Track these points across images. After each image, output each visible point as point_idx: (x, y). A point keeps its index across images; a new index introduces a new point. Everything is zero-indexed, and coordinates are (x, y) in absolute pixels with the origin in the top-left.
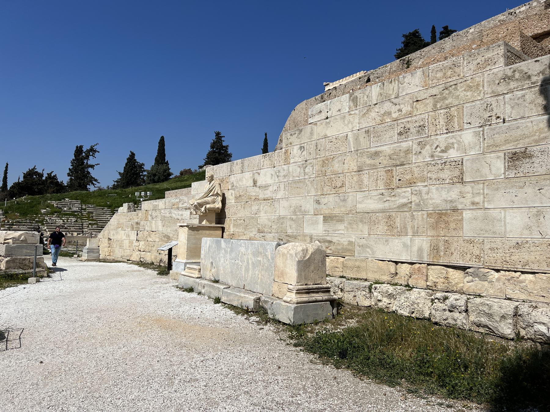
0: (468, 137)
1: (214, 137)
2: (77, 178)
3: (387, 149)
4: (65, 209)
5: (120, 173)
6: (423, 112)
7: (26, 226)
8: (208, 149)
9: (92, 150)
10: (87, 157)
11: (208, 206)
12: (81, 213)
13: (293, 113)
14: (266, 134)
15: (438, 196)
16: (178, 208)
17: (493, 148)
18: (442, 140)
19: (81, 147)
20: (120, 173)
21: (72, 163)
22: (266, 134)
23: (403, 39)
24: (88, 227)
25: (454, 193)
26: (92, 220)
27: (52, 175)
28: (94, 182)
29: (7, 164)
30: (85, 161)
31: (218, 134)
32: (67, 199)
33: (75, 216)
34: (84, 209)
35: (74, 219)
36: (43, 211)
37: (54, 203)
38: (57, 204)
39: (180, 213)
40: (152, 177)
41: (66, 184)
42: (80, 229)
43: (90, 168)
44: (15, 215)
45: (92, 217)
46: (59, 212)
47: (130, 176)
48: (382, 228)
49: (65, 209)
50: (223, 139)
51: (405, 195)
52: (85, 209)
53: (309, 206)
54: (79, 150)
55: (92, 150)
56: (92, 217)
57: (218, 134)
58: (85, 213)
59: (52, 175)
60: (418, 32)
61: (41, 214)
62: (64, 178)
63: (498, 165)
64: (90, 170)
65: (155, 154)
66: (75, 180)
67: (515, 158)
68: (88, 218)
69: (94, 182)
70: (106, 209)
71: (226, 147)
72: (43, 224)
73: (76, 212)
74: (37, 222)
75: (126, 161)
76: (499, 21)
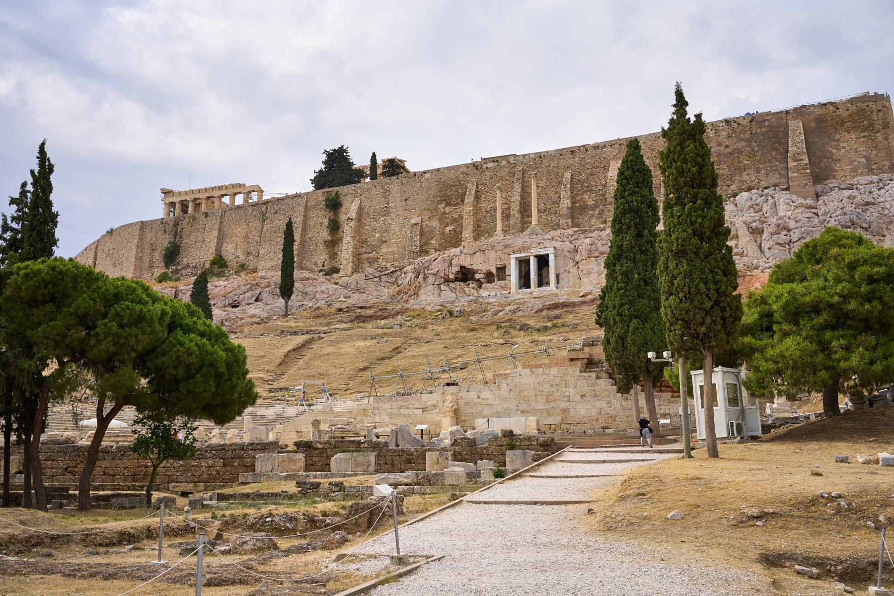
0: (571, 389)
3: (546, 390)
6: (558, 380)
15: (563, 405)
17: (577, 393)
18: (564, 389)
23: (324, 157)
25: (568, 404)
48: (545, 414)
51: (553, 404)
53: (513, 407)
60: (345, 151)
63: (579, 398)
67: (583, 396)
76: (462, 173)
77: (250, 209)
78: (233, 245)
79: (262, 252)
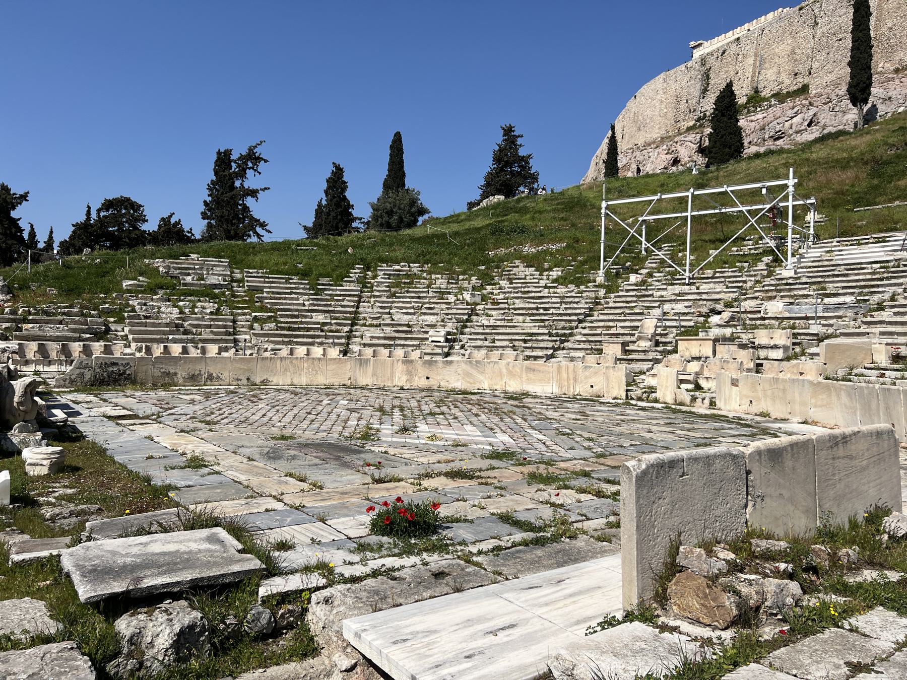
1: (499, 138)
2: (220, 219)
4: (189, 279)
5: (305, 228)
7: (67, 324)
8: (487, 164)
9: (252, 158)
10: (242, 174)
12: (231, 289)
13: (632, 105)
19: (228, 153)
20: (305, 228)
21: (209, 189)
24: (251, 328)
26: (263, 309)
27: (173, 221)
28: (259, 230)
29: (89, 207)
30: (237, 184)
31: (508, 131)
32: (193, 256)
33: (213, 297)
34: (238, 281)
35: (210, 307)
36: (126, 284)
37: (160, 265)
38: (168, 267)
40: (386, 218)
41: (198, 237)
42: (230, 334)
43: (249, 198)
44: (44, 294)
45: (261, 300)
46: (172, 288)
47: (335, 218)
49: (189, 279)
50: (519, 141)
52: (241, 281)
54: (223, 160)
55: (252, 158)
56: (261, 300)
57: (508, 131)
58: (240, 291)
59: (173, 221)
61: (120, 291)
62: (196, 225)
64: (250, 201)
65: (384, 173)
66: (219, 226)
68: (250, 304)
69: (259, 230)
70: (295, 279)
71: (526, 159)
72: (121, 320)
73: (215, 286)
74: (102, 313)
75: (325, 186)
78: (775, 70)
79: (816, 65)
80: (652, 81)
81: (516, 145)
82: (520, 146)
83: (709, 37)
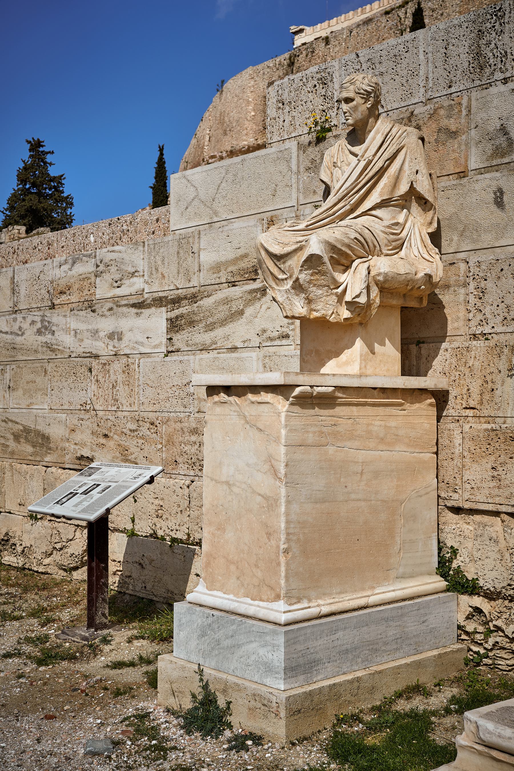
1: (25, 154)
8: (12, 185)
11: (382, 265)
14: (161, 149)
16: (91, 306)
22: (161, 149)
31: (36, 146)
39: (106, 325)
50: (49, 158)
57: (36, 146)
77: (384, 19)
80: (239, 75)
81: (45, 163)
82: (51, 164)
83: (312, 23)
